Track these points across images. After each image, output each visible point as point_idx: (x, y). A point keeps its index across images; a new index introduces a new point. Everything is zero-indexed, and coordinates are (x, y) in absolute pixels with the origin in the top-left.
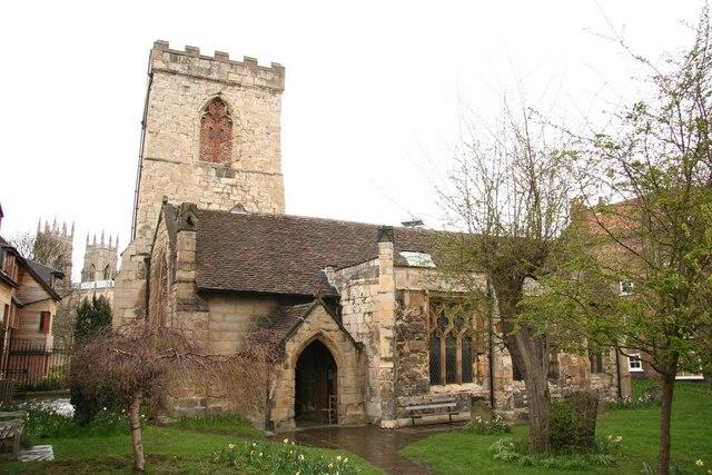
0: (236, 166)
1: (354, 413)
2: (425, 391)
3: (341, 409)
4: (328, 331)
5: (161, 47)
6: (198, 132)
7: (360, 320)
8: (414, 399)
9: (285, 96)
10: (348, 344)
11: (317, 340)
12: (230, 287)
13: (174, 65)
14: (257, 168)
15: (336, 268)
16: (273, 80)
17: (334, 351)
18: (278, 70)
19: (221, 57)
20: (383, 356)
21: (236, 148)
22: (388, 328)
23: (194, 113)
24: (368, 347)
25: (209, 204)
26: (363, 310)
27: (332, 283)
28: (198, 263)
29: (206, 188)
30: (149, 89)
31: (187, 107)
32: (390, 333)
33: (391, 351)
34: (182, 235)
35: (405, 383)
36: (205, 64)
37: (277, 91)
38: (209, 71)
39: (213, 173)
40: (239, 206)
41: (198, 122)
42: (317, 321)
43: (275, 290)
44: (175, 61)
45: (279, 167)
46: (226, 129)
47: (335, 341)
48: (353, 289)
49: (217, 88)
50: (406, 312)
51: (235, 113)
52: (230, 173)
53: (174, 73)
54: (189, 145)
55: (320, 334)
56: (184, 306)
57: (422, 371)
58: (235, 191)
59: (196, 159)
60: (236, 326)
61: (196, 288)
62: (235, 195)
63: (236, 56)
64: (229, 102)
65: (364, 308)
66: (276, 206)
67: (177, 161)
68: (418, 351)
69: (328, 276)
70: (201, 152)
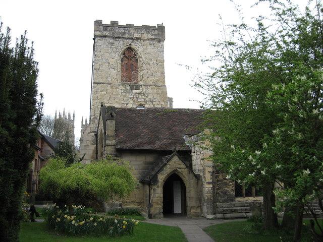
0: (141, 83)
2: (232, 200)
4: (180, 168)
5: (98, 23)
6: (120, 66)
8: (225, 204)
9: (166, 43)
10: (191, 175)
12: (132, 147)
13: (105, 32)
25: (127, 104)
28: (116, 136)
31: (113, 54)
32: (211, 169)
34: (108, 122)
35: (221, 196)
36: (121, 30)
38: (124, 34)
39: (128, 88)
40: (141, 105)
42: (175, 163)
43: (157, 148)
45: (164, 82)
49: (129, 42)
53: (105, 36)
54: (115, 74)
55: (176, 170)
57: (230, 189)
58: (140, 97)
59: (119, 81)
67: (110, 82)
69: (186, 140)
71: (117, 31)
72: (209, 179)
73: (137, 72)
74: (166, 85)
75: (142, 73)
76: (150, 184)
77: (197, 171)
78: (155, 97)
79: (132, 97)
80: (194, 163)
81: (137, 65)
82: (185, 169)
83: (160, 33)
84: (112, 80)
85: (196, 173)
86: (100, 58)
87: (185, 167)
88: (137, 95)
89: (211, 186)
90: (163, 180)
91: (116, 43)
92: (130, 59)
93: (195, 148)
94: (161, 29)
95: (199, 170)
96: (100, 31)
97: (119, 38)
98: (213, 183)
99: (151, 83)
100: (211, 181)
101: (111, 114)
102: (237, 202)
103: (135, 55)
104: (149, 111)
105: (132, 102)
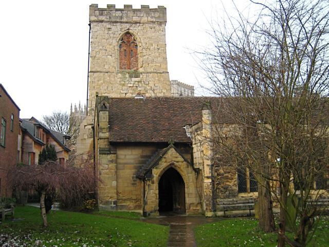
0: (141, 70)
1: (195, 208)
3: (187, 206)
4: (177, 162)
5: (94, 8)
6: (117, 53)
7: (200, 156)
8: (226, 201)
9: (168, 27)
10: (190, 169)
11: (172, 168)
13: (102, 17)
16: (159, 17)
17: (181, 173)
19: (128, 7)
21: (140, 60)
23: (115, 43)
25: (126, 94)
27: (188, 135)
28: (110, 129)
30: (90, 33)
32: (209, 162)
35: (221, 191)
37: (162, 22)
39: (127, 76)
42: (172, 156)
43: (153, 140)
44: (101, 14)
46: (134, 49)
49: (128, 26)
51: (138, 39)
53: (102, 21)
54: (112, 61)
55: (173, 164)
56: (103, 152)
57: (233, 184)
59: (118, 69)
60: (132, 161)
62: (140, 87)
63: (136, 6)
67: (107, 71)
68: (229, 172)
71: (114, 15)
72: (208, 173)
76: (144, 180)
77: (198, 164)
79: (132, 85)
83: (161, 15)
84: (109, 68)
85: (195, 167)
87: (183, 160)
88: (137, 83)
89: (210, 180)
90: (158, 174)
91: (113, 28)
92: (128, 42)
94: (162, 10)
96: (95, 16)
97: (116, 22)
98: (212, 177)
99: (152, 70)
100: (210, 175)
101: (104, 104)
102: (240, 198)
104: (149, 100)
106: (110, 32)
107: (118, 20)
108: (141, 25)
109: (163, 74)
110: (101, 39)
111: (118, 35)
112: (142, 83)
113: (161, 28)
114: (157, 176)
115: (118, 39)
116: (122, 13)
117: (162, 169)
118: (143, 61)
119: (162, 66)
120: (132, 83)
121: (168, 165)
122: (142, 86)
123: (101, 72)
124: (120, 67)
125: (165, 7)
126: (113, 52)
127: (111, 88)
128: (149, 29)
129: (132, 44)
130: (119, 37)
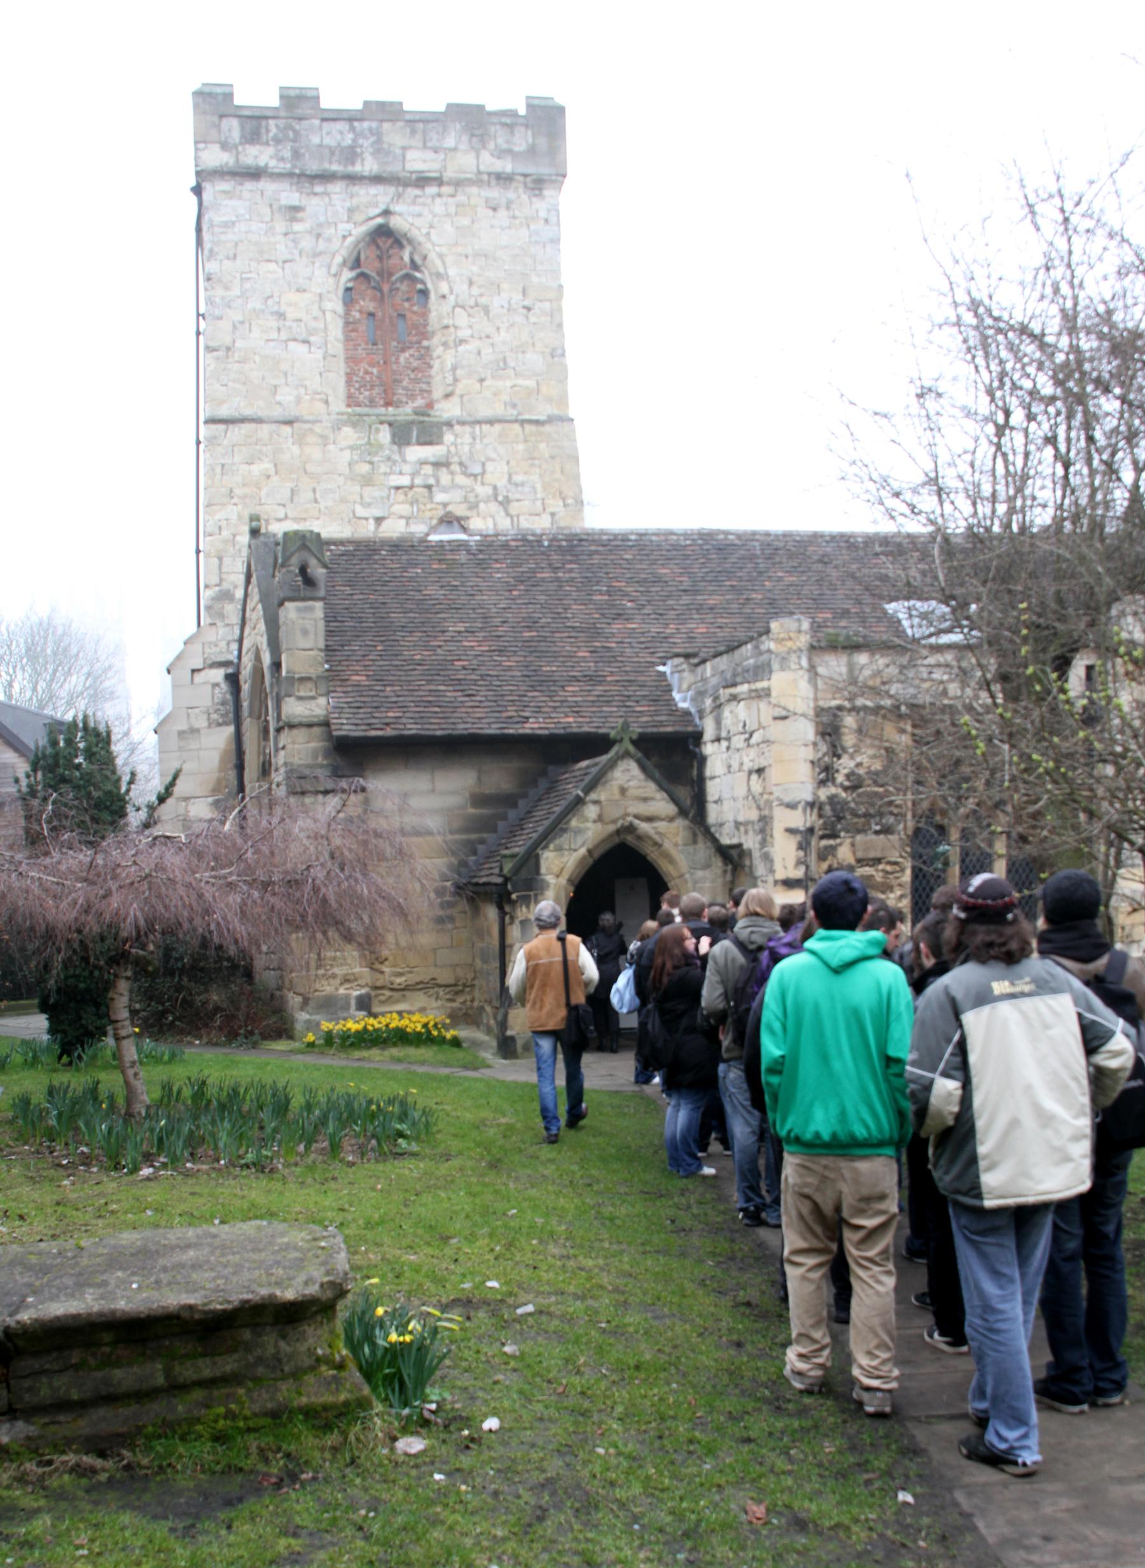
0: (448, 410)
4: (650, 819)
5: (213, 103)
6: (336, 330)
7: (741, 791)
9: (570, 198)
10: (703, 849)
12: (412, 729)
14: (499, 410)
15: (693, 658)
18: (546, 119)
20: (780, 875)
21: (443, 359)
22: (792, 806)
24: (756, 854)
25: (379, 520)
26: (748, 765)
28: (332, 679)
29: (367, 481)
32: (799, 819)
33: (799, 862)
34: (290, 611)
38: (351, 154)
39: (384, 435)
41: (335, 305)
43: (528, 728)
44: (253, 136)
45: (563, 400)
47: (667, 845)
48: (726, 712)
49: (379, 197)
50: (845, 765)
52: (422, 429)
53: (255, 174)
55: (630, 829)
59: (339, 405)
61: (330, 736)
62: (445, 490)
63: (424, 97)
64: (415, 233)
65: (750, 759)
66: (556, 505)
67: (293, 412)
68: (878, 861)
69: (674, 680)
70: (349, 382)
71: (316, 140)
72: (791, 862)
73: (425, 356)
74: (571, 415)
75: (449, 358)
77: (728, 828)
78: (518, 478)
79: (405, 481)
80: (713, 790)
81: (425, 314)
82: (671, 819)
83: (542, 142)
84: (298, 400)
85: (726, 841)
86: (236, 291)
87: (670, 809)
88: (428, 470)
92: (386, 282)
93: (718, 722)
95: (737, 825)
96: (225, 146)
97: (326, 177)
103: (414, 266)
105: (405, 509)
106: (297, 227)
107: (335, 167)
108: (445, 190)
109: (547, 428)
110: (259, 262)
111: (336, 244)
112: (455, 468)
113: (541, 206)
114: (563, 881)
115: (339, 259)
116: (352, 129)
117: (583, 851)
118: (454, 369)
119: (544, 389)
120: (407, 468)
121: (611, 836)
122: (454, 486)
123: (258, 421)
124: (350, 396)
125: (560, 100)
126: (314, 324)
127: (311, 495)
128: (483, 212)
129: (404, 287)
130: (344, 252)
